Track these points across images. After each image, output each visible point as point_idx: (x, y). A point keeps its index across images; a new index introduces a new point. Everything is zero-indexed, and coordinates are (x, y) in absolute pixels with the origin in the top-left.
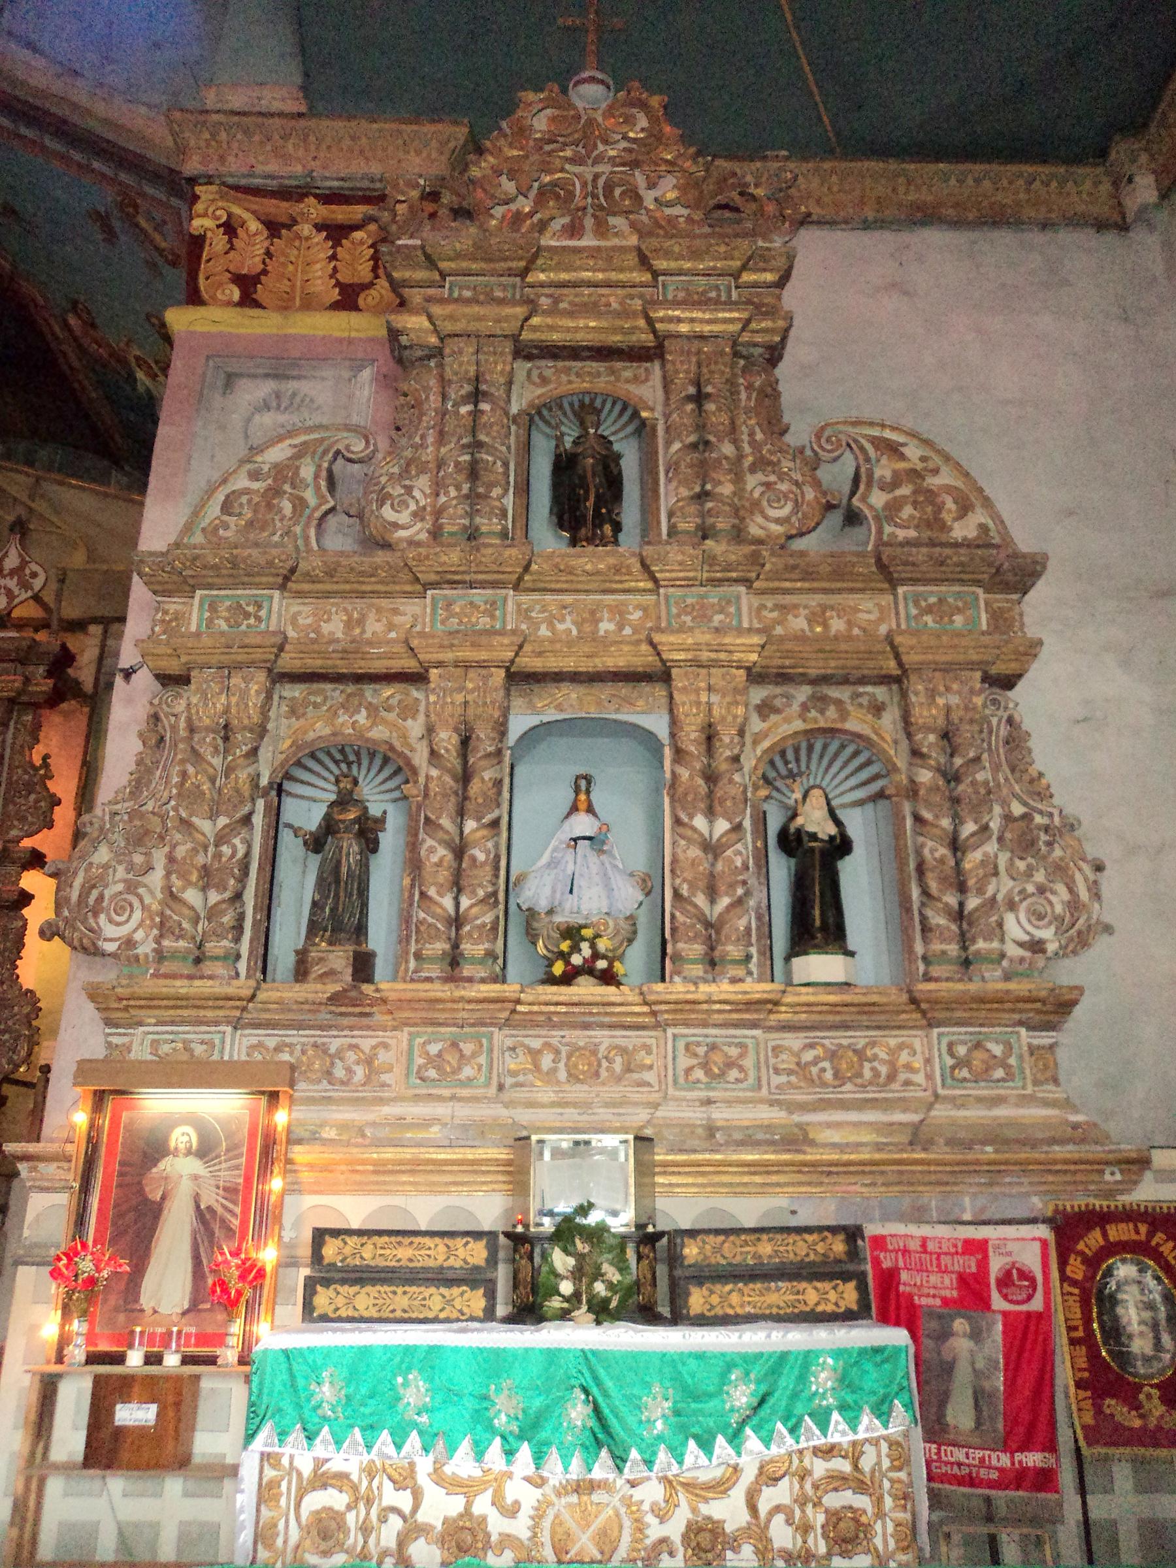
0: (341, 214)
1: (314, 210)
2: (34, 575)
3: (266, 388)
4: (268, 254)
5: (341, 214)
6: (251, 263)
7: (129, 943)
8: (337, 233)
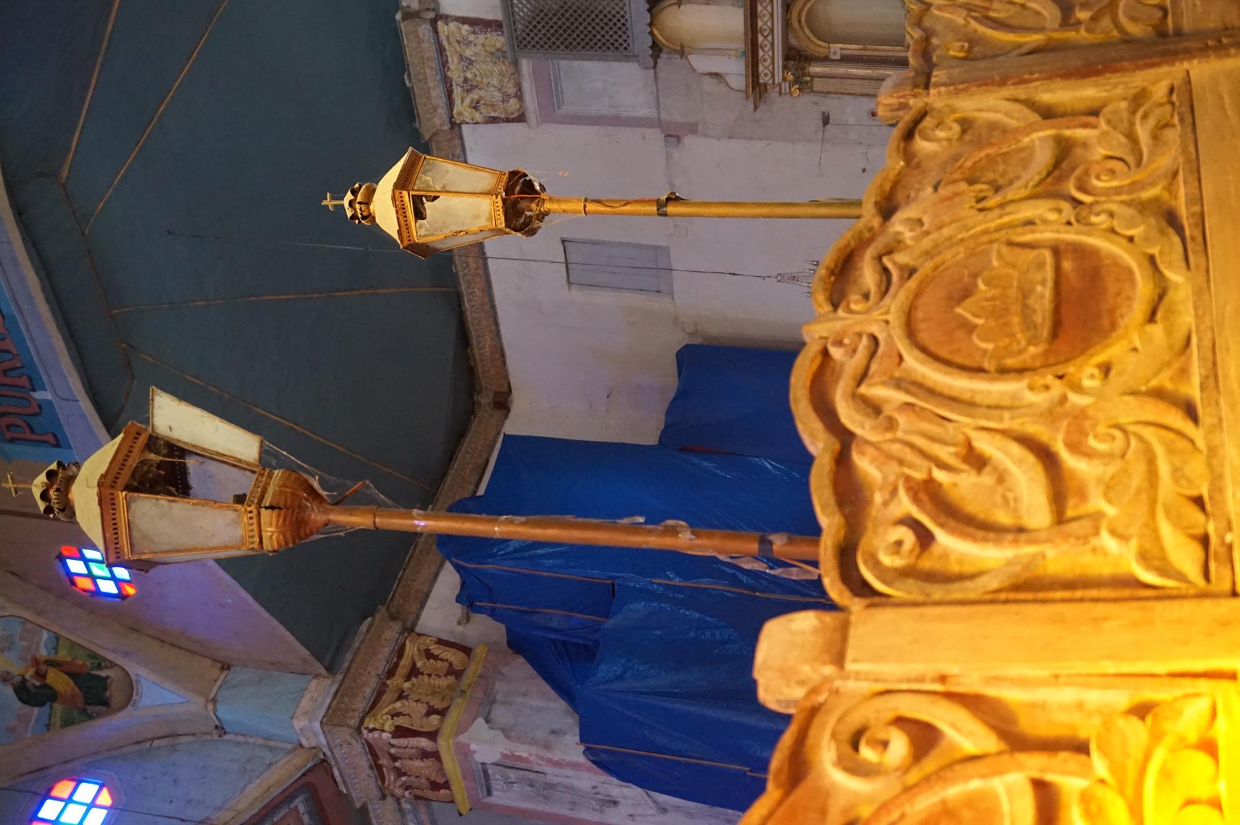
1: (397, 681)
6: (423, 709)
8: (414, 672)
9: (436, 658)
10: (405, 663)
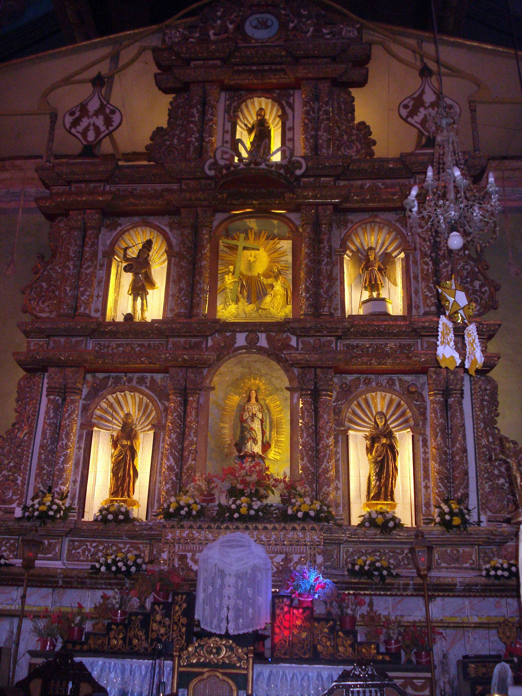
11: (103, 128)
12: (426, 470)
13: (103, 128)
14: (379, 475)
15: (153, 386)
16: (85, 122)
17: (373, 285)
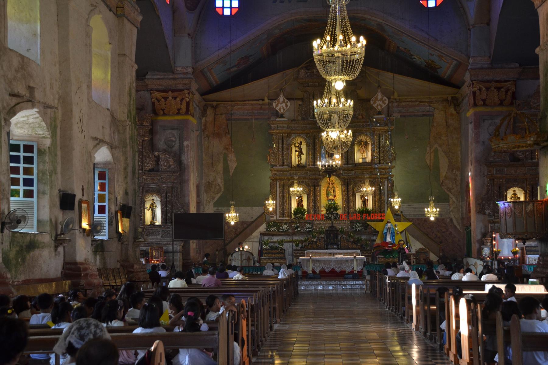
0: (499, 85)
2: (385, 100)
3: (490, 121)
4: (487, 95)
5: (499, 85)
6: (484, 97)
7: (489, 213)
8: (498, 89)
9: (506, 94)
10: (503, 84)
11: (285, 108)
12: (375, 203)
13: (285, 108)
14: (363, 205)
15: (306, 184)
16: (280, 106)
17: (363, 152)
